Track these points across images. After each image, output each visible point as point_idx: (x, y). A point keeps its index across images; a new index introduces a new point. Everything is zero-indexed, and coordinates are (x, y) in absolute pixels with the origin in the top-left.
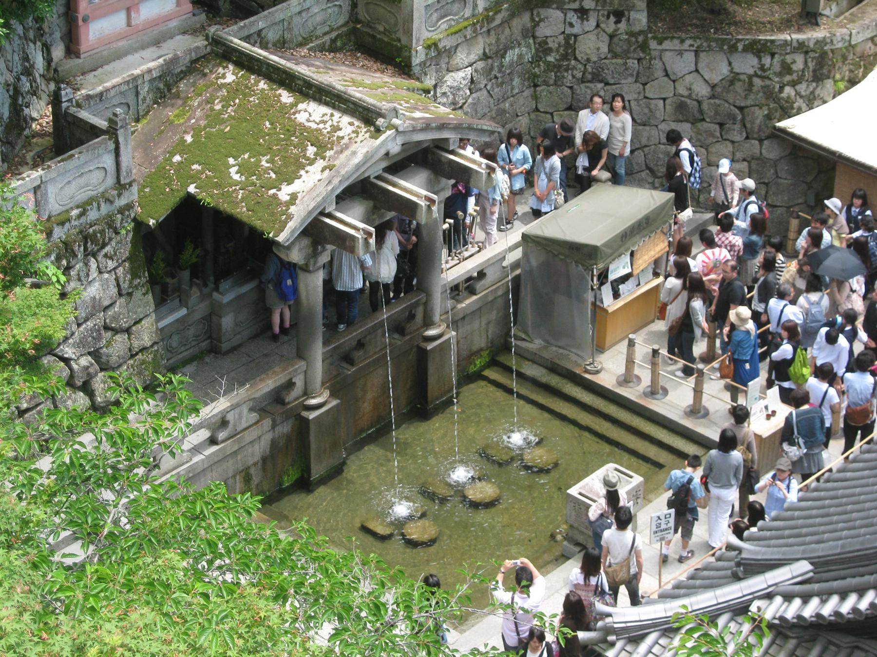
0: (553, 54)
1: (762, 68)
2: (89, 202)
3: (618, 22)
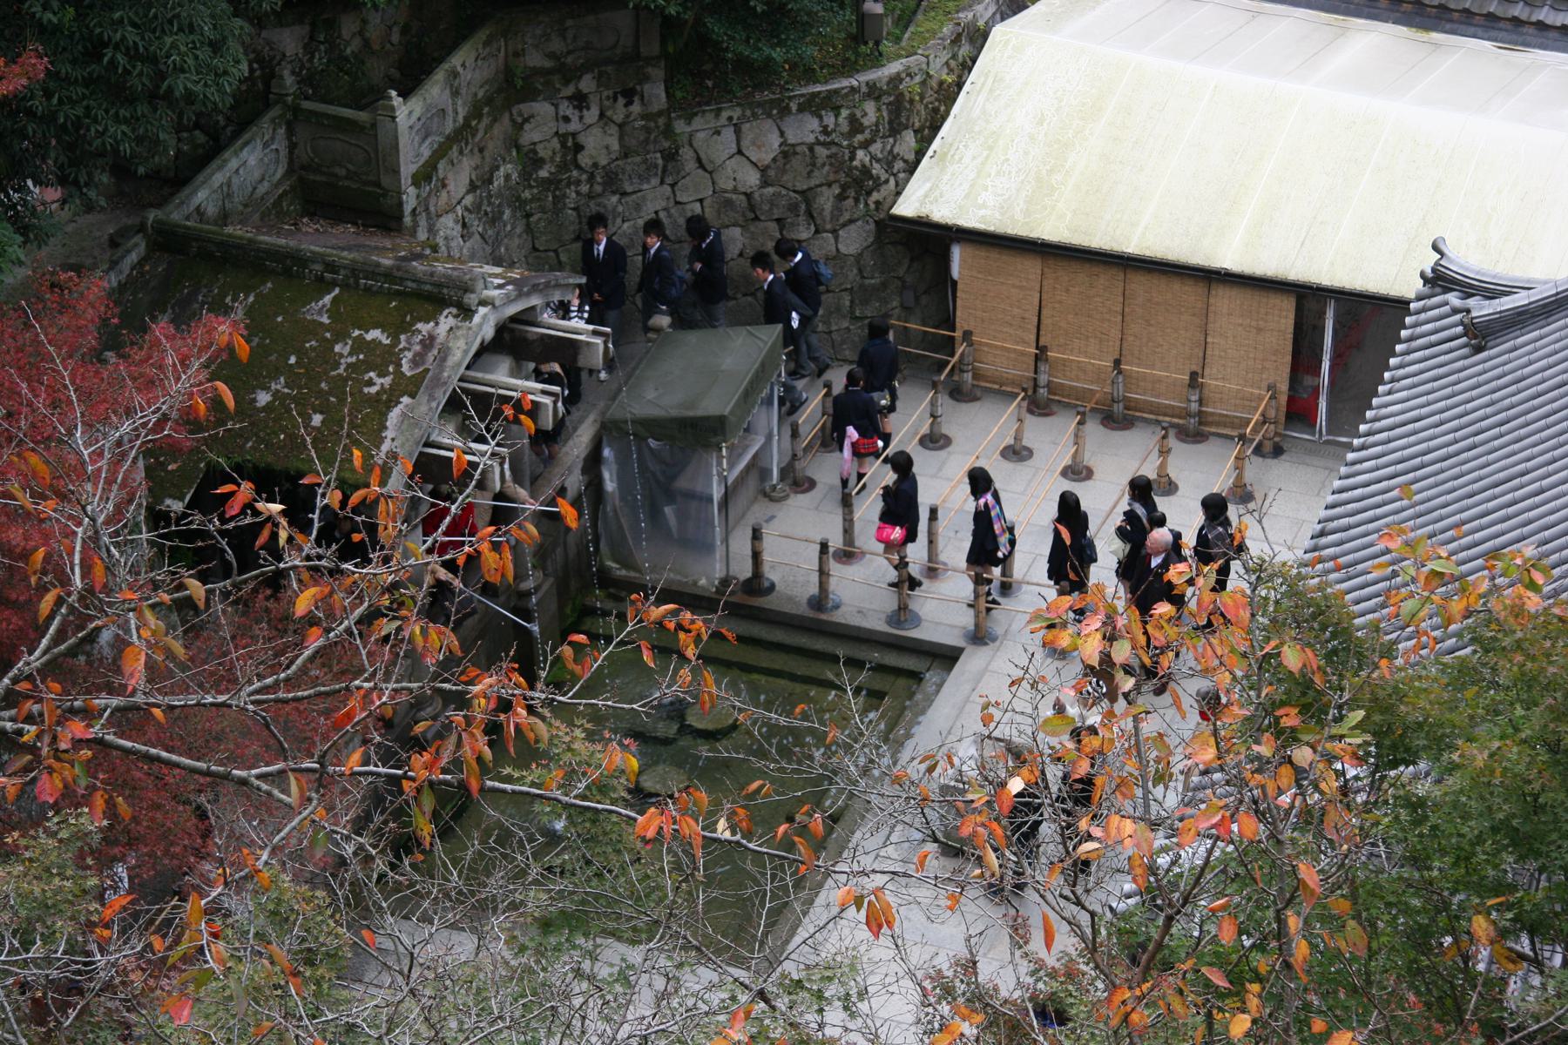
0: (547, 167)
1: (825, 131)
3: (626, 105)
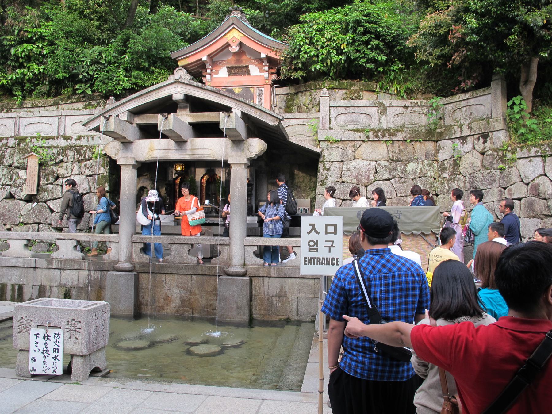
3: (484, 143)
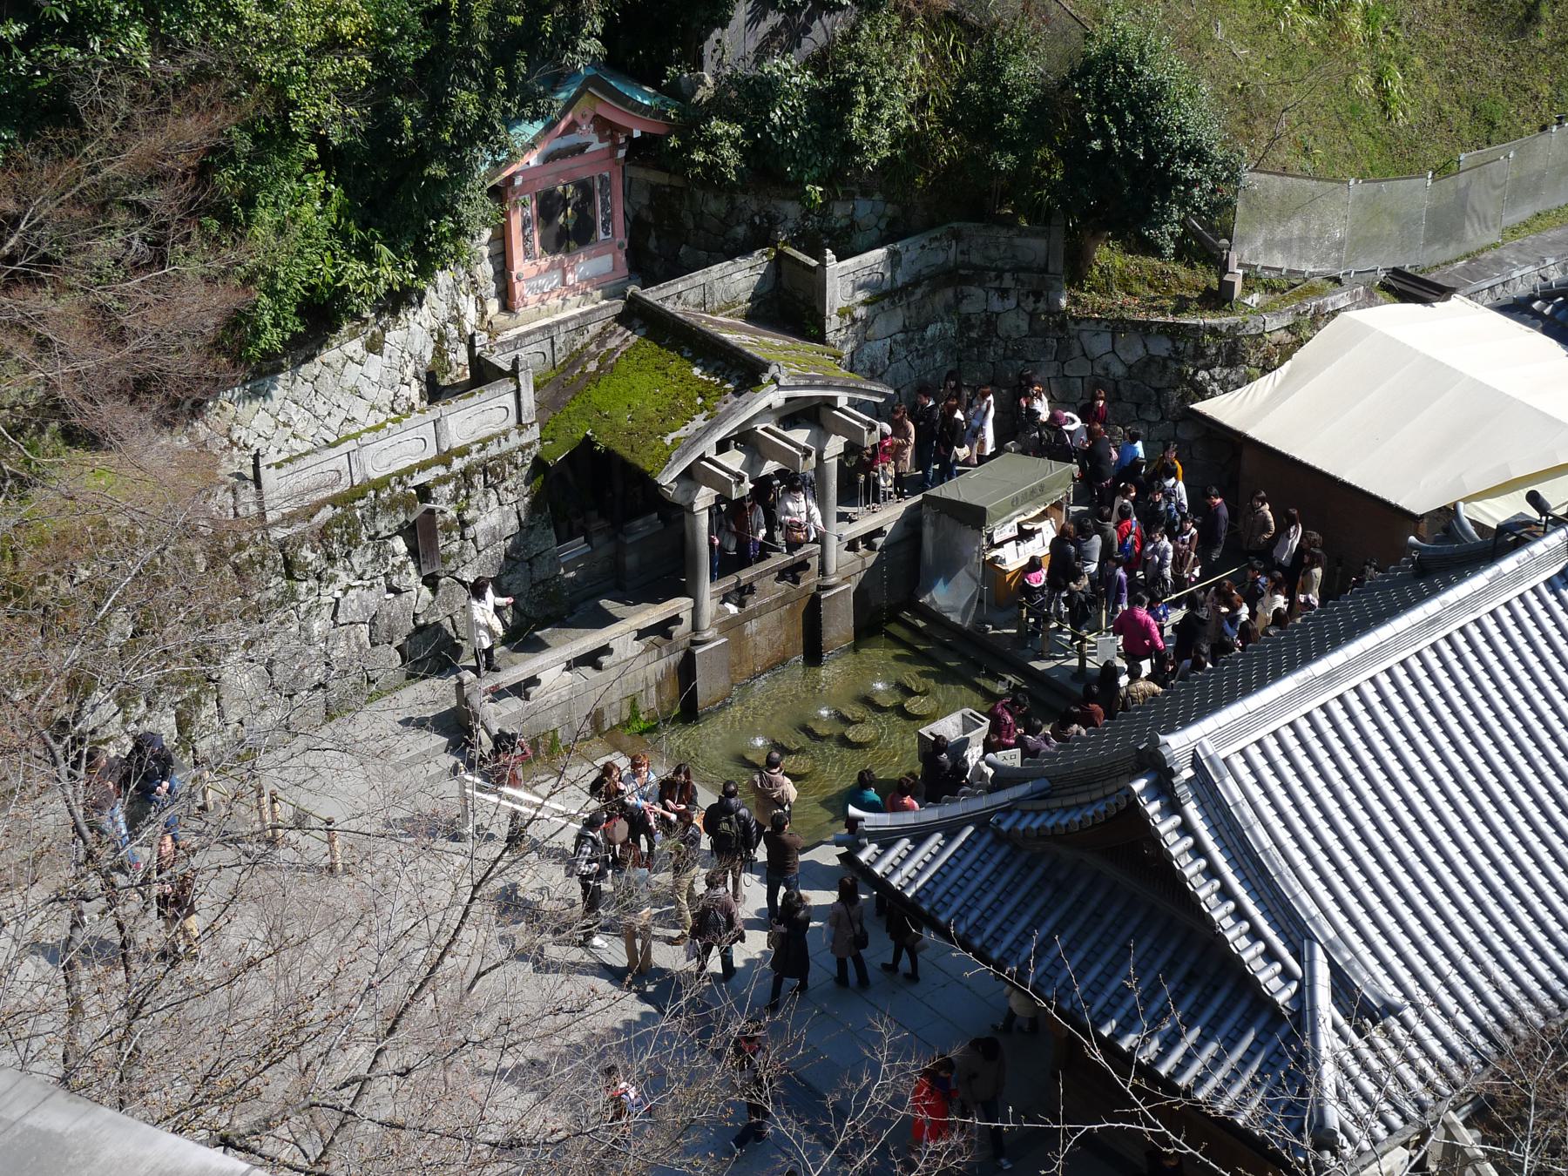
2: (490, 438)
